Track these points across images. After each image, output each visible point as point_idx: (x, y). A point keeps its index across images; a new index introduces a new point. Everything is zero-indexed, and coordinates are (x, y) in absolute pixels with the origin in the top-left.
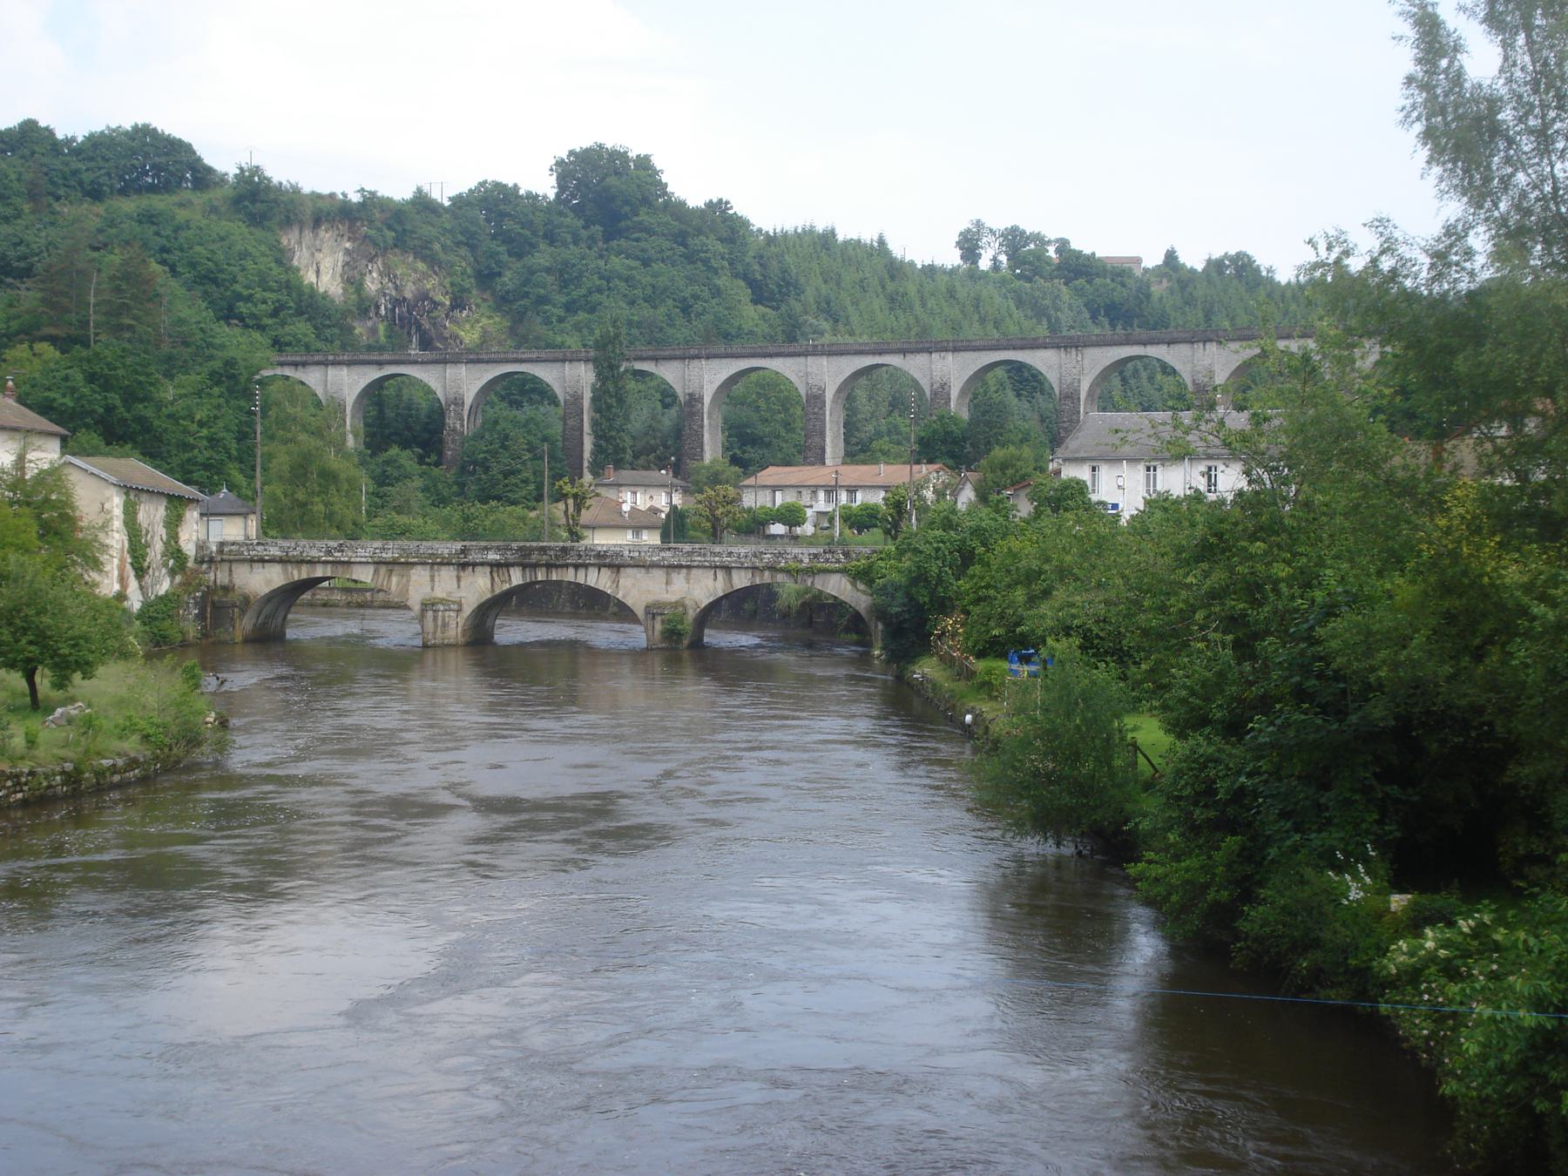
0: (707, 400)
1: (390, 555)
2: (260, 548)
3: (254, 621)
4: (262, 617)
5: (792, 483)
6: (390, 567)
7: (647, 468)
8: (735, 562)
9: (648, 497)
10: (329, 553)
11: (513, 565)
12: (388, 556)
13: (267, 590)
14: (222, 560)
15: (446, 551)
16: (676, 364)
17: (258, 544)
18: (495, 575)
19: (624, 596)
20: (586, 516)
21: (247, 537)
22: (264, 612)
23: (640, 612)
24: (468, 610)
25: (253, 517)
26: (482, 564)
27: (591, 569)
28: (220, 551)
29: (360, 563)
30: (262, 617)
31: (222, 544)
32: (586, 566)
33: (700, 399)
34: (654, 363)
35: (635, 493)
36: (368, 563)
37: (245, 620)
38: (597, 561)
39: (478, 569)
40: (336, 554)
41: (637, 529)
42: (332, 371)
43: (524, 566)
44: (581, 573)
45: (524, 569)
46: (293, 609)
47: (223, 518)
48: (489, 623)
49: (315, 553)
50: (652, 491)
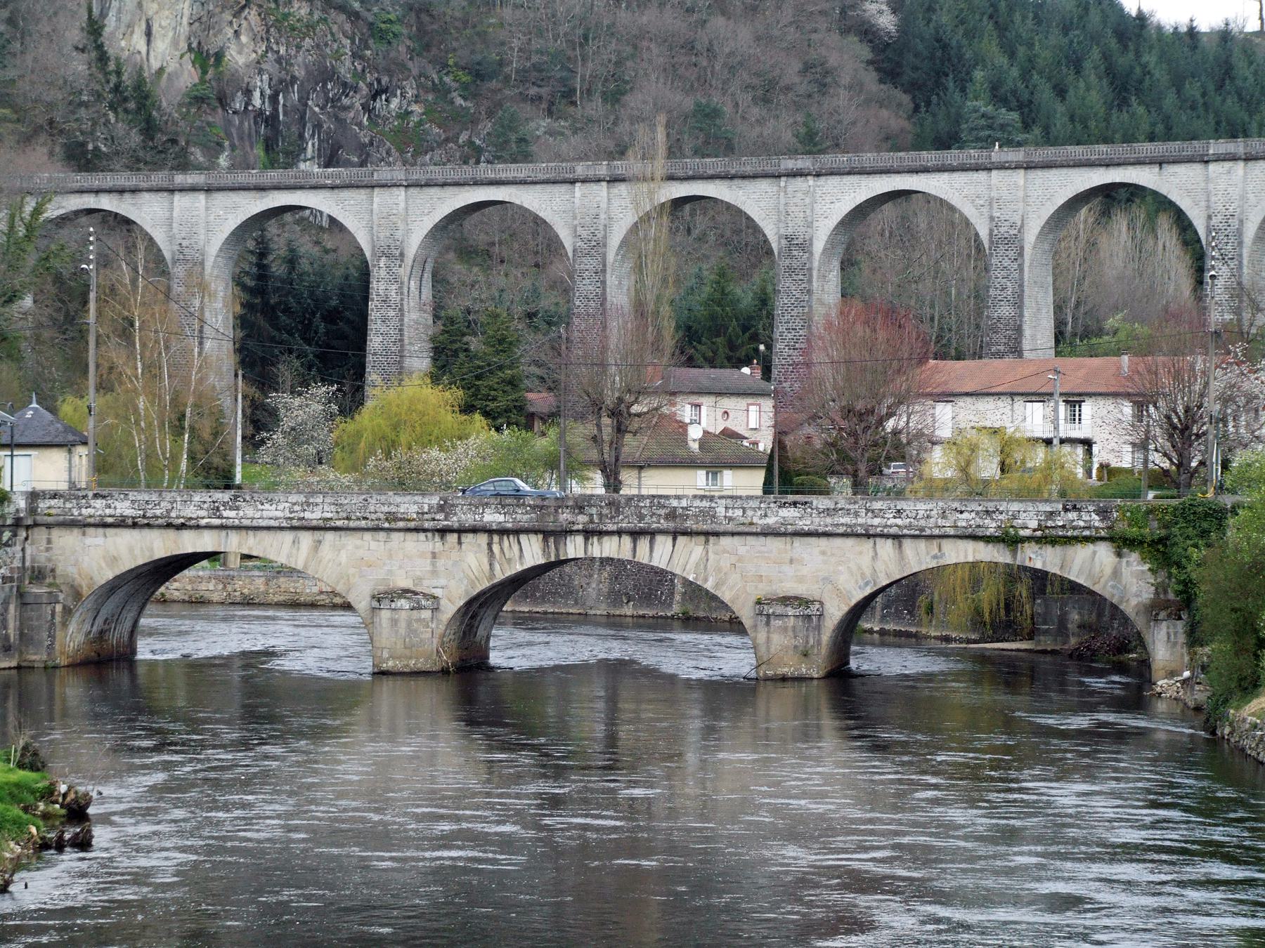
0: (819, 246)
1: (317, 515)
2: (99, 503)
3: (87, 627)
4: (100, 621)
5: (1020, 391)
6: (318, 534)
7: (712, 363)
8: (910, 527)
9: (719, 413)
10: (216, 512)
11: (527, 531)
12: (313, 516)
13: (110, 575)
14: (36, 525)
15: (414, 508)
16: (764, 185)
17: (96, 496)
18: (496, 548)
19: (717, 586)
20: (631, 445)
21: (72, 485)
22: (104, 613)
23: (746, 614)
24: (450, 608)
25: (82, 450)
26: (474, 530)
27: (660, 539)
28: (32, 510)
29: (269, 528)
30: (100, 621)
31: (34, 496)
32: (652, 534)
33: (806, 246)
34: (1156, 169)
35: (698, 406)
36: (281, 528)
37: (72, 627)
38: (671, 525)
39: (468, 538)
40: (226, 514)
41: (715, 466)
42: (379, 196)
43: (546, 534)
44: (643, 543)
45: (545, 540)
46: (150, 608)
47: (33, 452)
48: (481, 632)
49: (190, 511)
50: (728, 403)
